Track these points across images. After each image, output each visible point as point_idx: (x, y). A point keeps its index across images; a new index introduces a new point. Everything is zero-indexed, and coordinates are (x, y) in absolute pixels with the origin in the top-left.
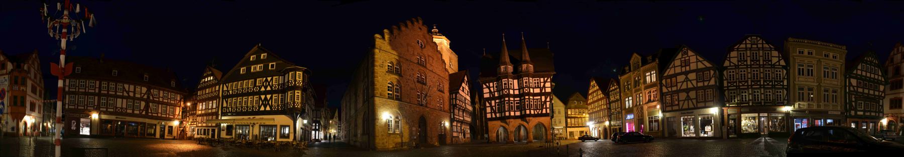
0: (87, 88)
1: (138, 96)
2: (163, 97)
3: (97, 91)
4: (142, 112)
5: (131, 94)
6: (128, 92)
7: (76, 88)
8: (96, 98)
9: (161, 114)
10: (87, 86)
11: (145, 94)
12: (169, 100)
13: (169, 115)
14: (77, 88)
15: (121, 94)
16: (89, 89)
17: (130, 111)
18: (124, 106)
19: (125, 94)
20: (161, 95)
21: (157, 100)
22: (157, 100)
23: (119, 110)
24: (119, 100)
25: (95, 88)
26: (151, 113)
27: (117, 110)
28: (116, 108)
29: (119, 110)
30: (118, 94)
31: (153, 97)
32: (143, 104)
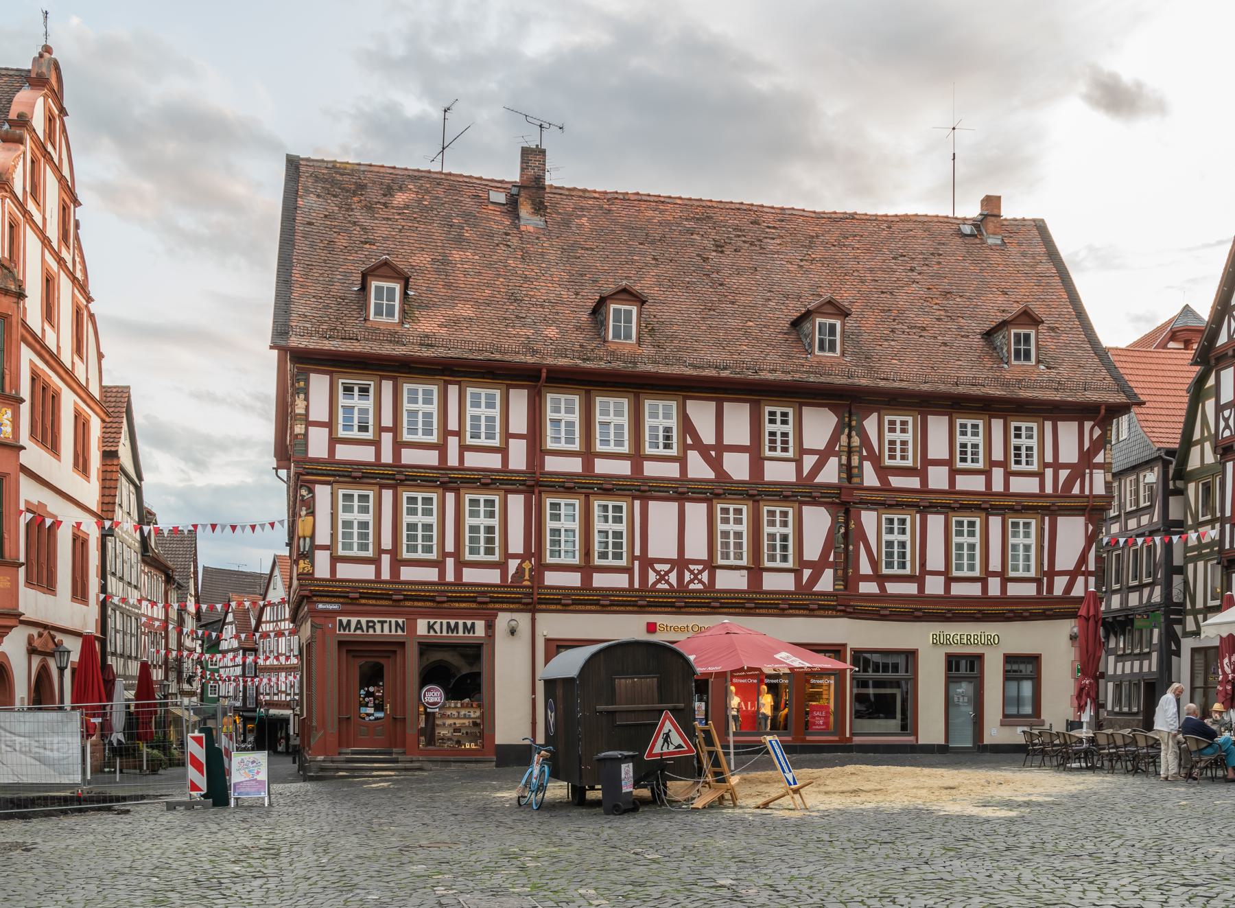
0: (453, 442)
1: (779, 472)
2: (949, 463)
3: (518, 458)
4: (815, 579)
5: (737, 467)
6: (714, 454)
7: (376, 443)
8: (516, 503)
9: (949, 580)
10: (453, 425)
11: (824, 456)
12: (998, 473)
13: (1005, 580)
14: (387, 438)
15: (672, 471)
16: (463, 448)
17: (731, 581)
18: (697, 548)
19: (699, 468)
20: (938, 447)
21: (914, 483)
22: (914, 483)
23: (662, 577)
24: (662, 514)
25: (507, 436)
26: (881, 579)
27: (652, 577)
28: (647, 563)
29: (662, 577)
30: (651, 469)
31: (883, 472)
32: (817, 522)
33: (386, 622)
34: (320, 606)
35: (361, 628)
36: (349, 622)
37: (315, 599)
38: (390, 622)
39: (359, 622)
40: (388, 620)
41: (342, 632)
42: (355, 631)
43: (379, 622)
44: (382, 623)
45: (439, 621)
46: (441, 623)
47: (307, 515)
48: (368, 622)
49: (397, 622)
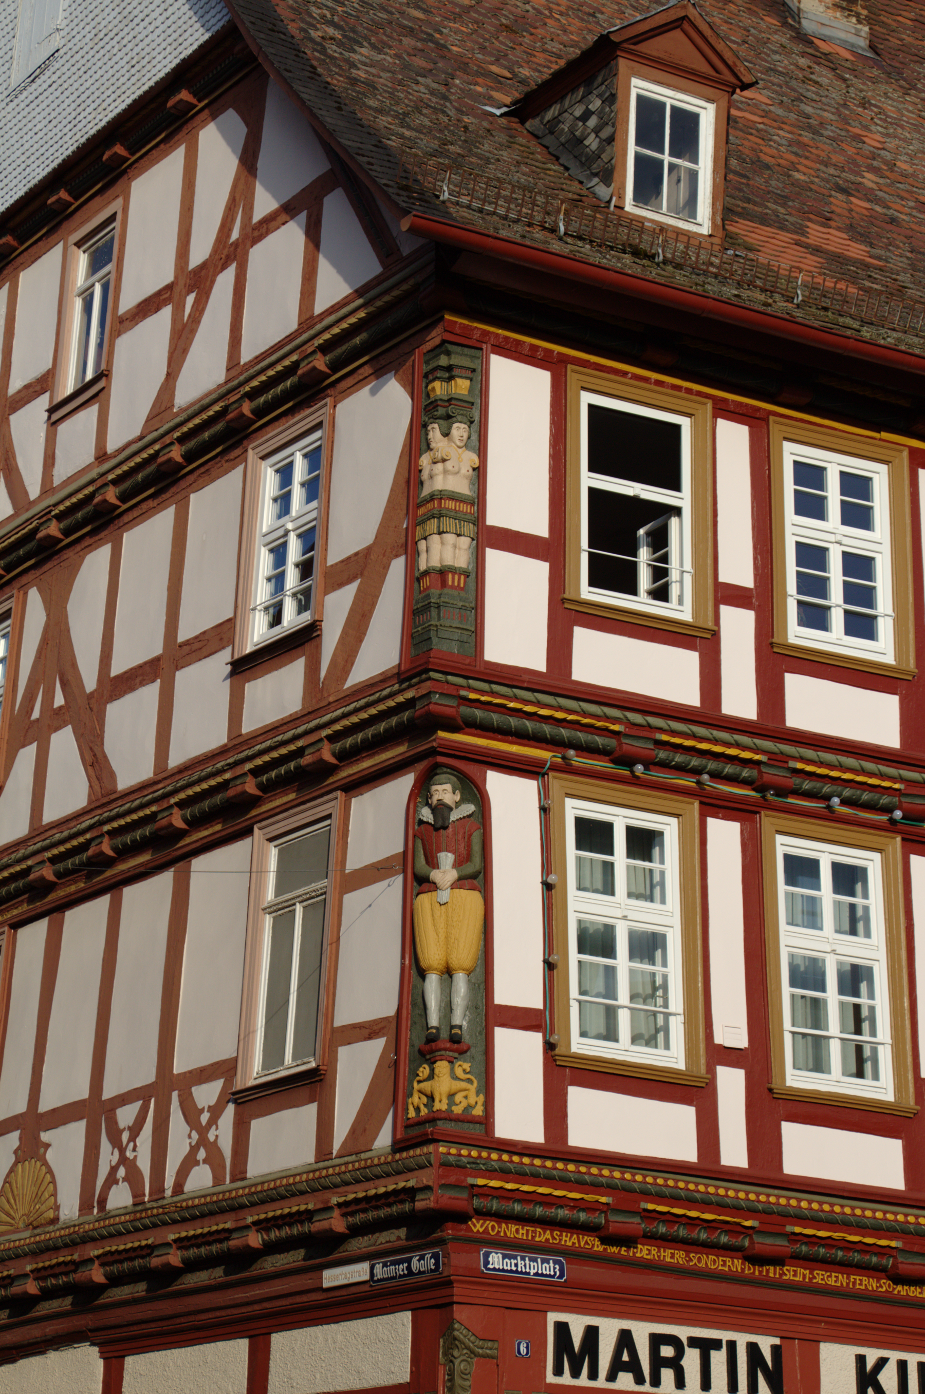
33: (716, 1344)
34: (496, 1260)
35: (634, 1367)
36: (592, 1334)
37: (478, 1226)
38: (732, 1345)
39: (625, 1339)
40: (725, 1336)
41: (566, 1379)
42: (612, 1377)
43: (694, 1342)
44: (706, 1346)
45: (894, 1356)
46: (902, 1366)
47: (460, 883)
48: (657, 1341)
49: (753, 1349)
